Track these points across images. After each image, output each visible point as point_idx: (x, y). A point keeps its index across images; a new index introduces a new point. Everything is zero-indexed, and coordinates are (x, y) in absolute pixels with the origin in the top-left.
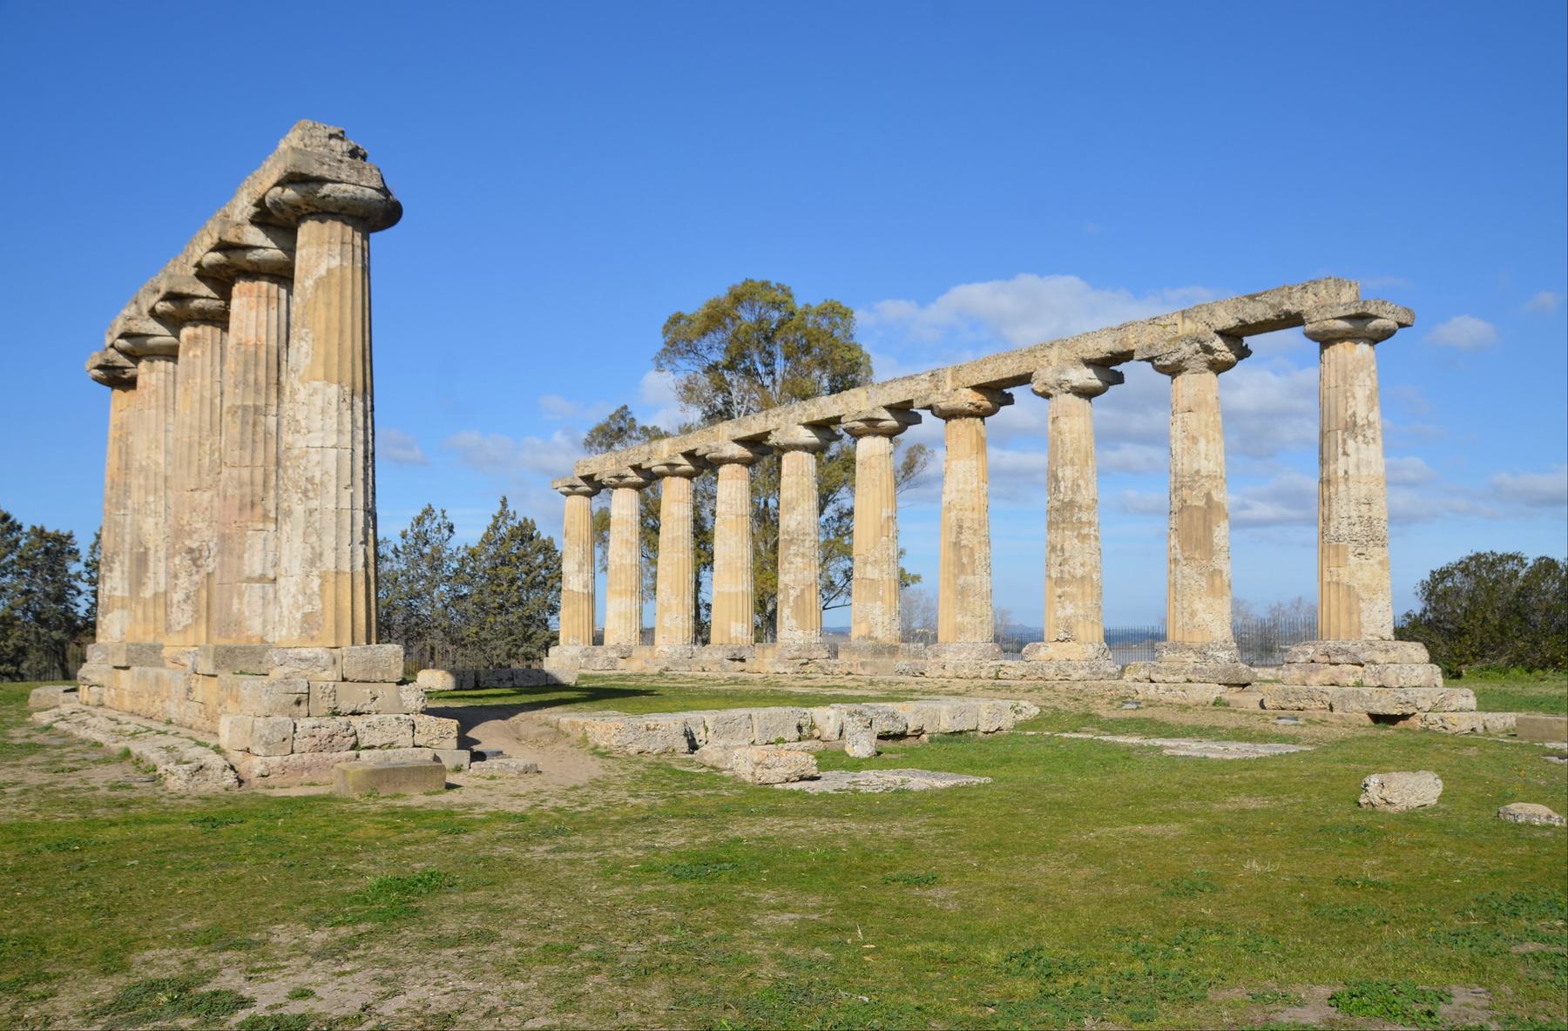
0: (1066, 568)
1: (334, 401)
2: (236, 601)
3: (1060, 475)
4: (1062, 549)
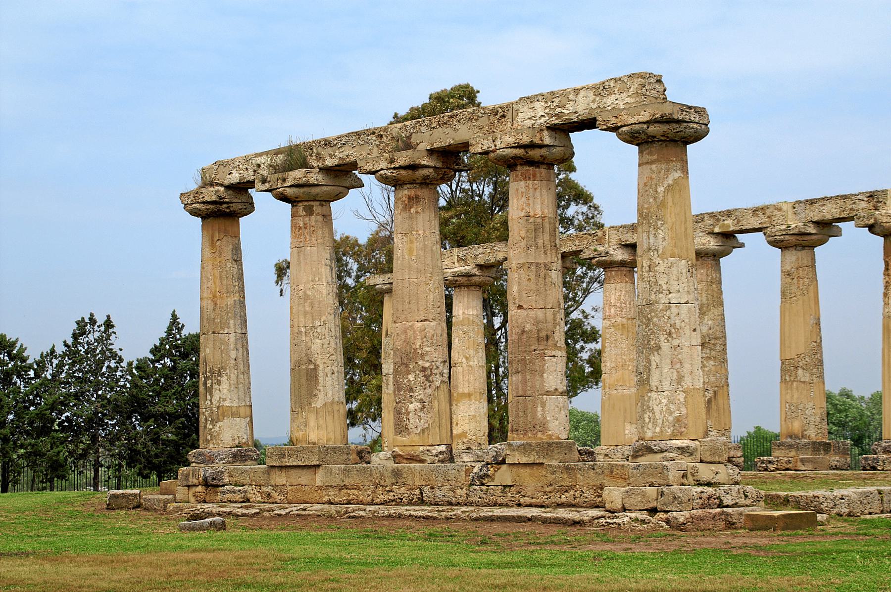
1: (684, 271)
2: (539, 409)
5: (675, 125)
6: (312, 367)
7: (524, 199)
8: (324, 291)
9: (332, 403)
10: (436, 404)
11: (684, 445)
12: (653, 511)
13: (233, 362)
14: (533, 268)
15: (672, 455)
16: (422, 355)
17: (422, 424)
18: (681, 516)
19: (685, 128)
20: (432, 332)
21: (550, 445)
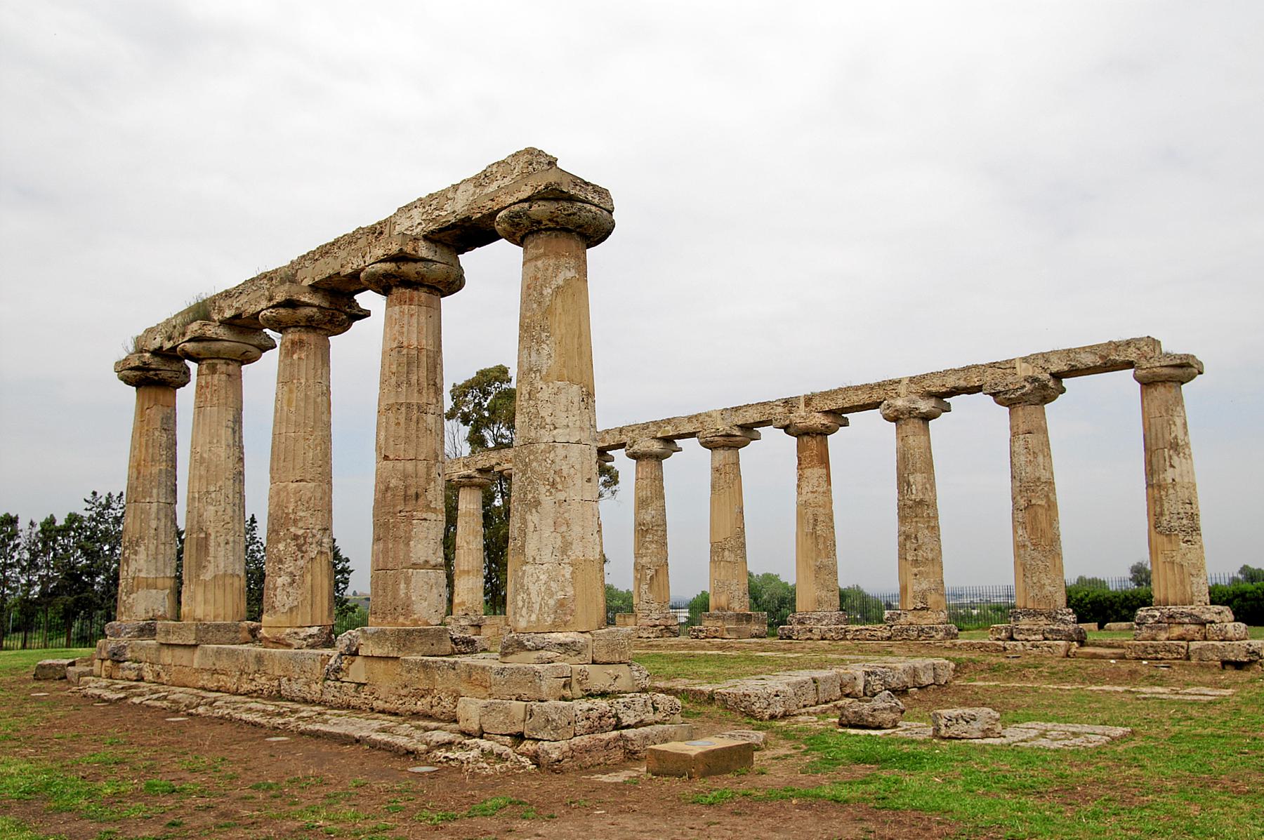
0: (920, 553)
1: (576, 400)
2: (402, 586)
3: (912, 480)
4: (916, 537)
5: (565, 204)
6: (203, 535)
7: (397, 327)
8: (223, 455)
9: (225, 575)
10: (309, 578)
11: (568, 640)
12: (519, 738)
13: (153, 532)
14: (403, 409)
15: (550, 654)
16: (295, 521)
17: (290, 602)
18: (553, 749)
19: (580, 210)
20: (309, 494)
21: (409, 633)
